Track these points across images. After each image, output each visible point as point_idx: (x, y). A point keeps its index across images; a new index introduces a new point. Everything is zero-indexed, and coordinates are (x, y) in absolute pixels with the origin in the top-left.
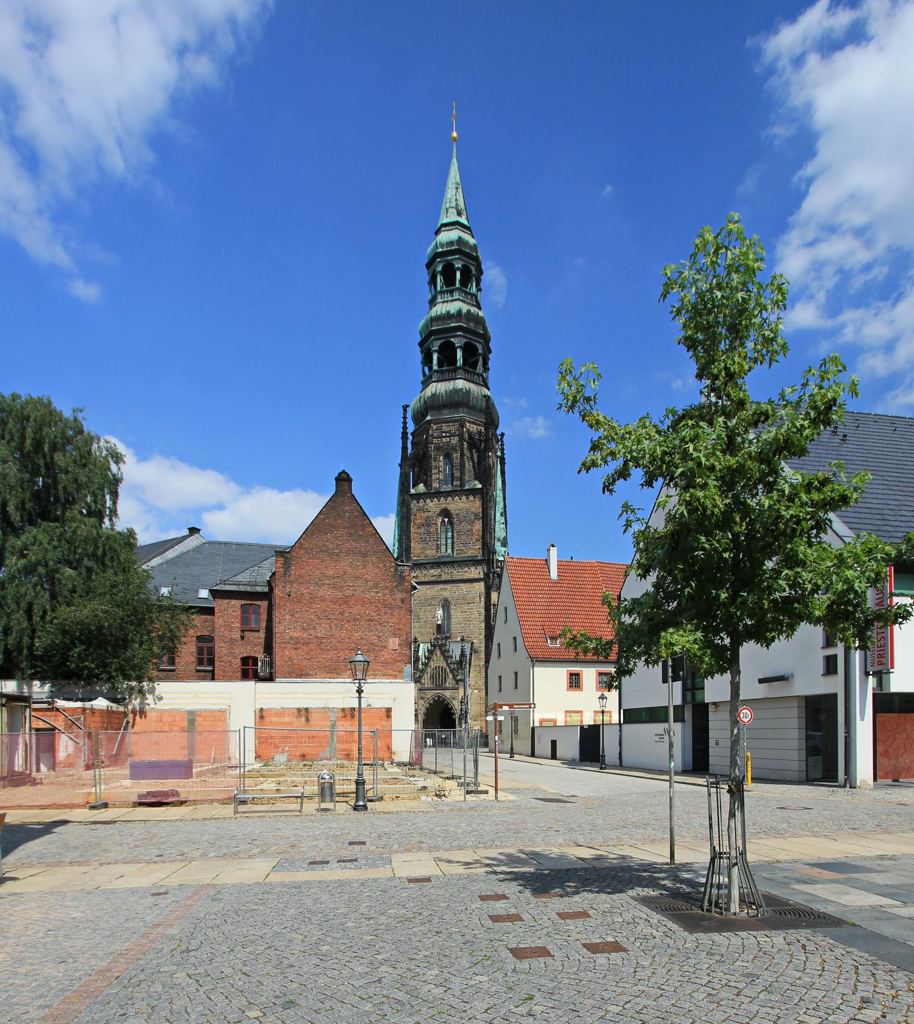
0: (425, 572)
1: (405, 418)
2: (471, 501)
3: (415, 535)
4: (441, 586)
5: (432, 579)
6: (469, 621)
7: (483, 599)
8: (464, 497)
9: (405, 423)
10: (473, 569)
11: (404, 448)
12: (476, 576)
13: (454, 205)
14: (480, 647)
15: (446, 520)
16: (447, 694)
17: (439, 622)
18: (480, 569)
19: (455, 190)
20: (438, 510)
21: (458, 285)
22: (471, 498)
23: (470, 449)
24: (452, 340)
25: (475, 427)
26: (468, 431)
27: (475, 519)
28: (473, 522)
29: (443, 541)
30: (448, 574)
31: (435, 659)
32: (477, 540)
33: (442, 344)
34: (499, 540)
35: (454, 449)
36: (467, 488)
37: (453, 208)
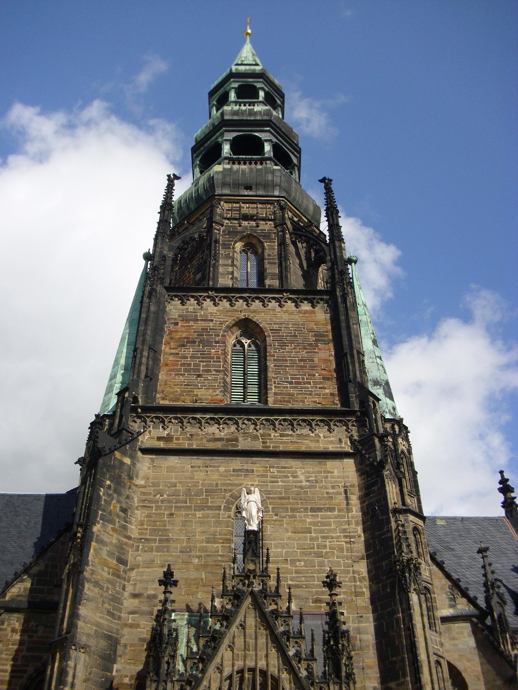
0: (189, 429)
2: (306, 312)
3: (171, 358)
4: (237, 463)
5: (211, 446)
7: (355, 500)
8: (290, 305)
10: (322, 432)
12: (331, 448)
14: (359, 631)
17: (254, 527)
18: (340, 432)
20: (230, 321)
21: (261, 99)
22: (306, 306)
23: (294, 244)
24: (257, 134)
27: (316, 340)
29: (238, 378)
30: (255, 438)
31: (239, 642)
32: (325, 379)
33: (237, 137)
35: (267, 236)
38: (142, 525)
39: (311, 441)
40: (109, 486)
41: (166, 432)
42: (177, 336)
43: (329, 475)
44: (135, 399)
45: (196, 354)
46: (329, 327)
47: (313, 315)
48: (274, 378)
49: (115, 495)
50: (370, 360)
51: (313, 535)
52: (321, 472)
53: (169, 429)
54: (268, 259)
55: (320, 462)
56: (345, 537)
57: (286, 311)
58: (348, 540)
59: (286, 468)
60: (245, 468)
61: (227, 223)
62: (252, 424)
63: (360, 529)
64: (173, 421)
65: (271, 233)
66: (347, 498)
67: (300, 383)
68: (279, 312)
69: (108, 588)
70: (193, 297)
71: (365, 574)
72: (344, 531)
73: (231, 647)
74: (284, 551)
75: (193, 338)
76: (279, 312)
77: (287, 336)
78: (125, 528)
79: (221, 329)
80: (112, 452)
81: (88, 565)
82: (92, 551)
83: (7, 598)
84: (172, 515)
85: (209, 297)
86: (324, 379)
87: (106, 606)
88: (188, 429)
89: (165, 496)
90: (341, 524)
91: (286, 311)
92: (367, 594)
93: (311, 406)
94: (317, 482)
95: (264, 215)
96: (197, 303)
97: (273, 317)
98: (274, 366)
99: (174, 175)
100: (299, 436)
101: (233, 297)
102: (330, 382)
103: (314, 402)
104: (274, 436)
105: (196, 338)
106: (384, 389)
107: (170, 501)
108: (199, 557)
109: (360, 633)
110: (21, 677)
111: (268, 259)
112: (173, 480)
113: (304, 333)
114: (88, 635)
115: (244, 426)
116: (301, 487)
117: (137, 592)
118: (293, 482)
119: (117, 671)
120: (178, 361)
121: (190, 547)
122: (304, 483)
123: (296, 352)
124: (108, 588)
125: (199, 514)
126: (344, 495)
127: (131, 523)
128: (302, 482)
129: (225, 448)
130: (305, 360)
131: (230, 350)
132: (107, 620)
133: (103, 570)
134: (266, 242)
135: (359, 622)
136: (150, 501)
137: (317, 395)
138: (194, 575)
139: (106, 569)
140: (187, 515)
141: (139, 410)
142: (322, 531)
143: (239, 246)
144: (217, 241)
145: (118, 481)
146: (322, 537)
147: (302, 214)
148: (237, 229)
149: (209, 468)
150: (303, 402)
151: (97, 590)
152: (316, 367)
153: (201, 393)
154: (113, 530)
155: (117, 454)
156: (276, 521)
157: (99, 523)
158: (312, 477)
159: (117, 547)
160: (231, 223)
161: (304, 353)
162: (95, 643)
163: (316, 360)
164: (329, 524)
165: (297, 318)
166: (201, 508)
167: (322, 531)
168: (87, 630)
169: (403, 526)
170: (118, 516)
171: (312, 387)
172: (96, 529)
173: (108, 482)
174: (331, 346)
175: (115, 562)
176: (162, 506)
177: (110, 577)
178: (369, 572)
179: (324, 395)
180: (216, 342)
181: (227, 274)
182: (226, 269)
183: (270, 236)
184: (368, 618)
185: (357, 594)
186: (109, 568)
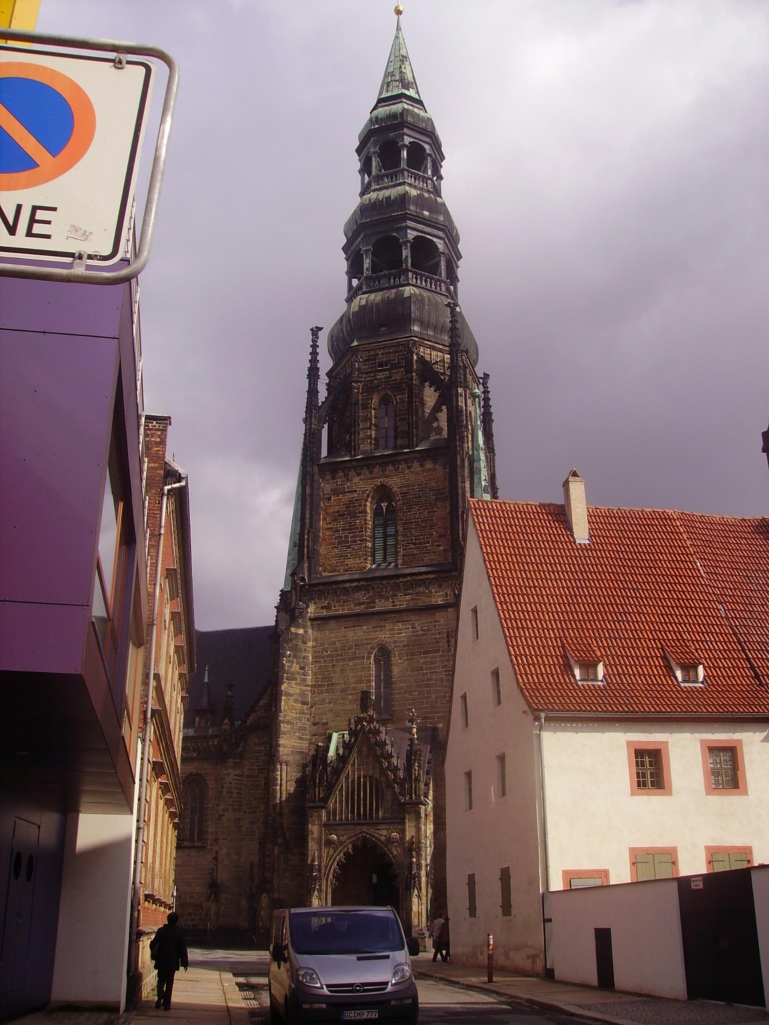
1: (314, 346)
2: (429, 470)
6: (428, 686)
8: (416, 464)
9: (314, 354)
11: (312, 392)
15: (384, 505)
16: (382, 833)
21: (403, 165)
22: (429, 465)
25: (434, 353)
26: (421, 359)
38: (316, 675)
40: (290, 654)
41: (327, 602)
42: (330, 511)
43: (437, 623)
44: (303, 579)
45: (345, 526)
46: (447, 484)
47: (434, 473)
48: (403, 541)
49: (295, 660)
52: (431, 622)
53: (328, 599)
54: (400, 415)
56: (445, 671)
57: (413, 472)
59: (407, 621)
60: (380, 624)
62: (385, 587)
64: (331, 591)
66: (448, 641)
67: (421, 543)
68: (407, 474)
69: (297, 722)
70: (341, 469)
73: (353, 765)
74: (405, 685)
75: (343, 511)
76: (407, 474)
77: (413, 498)
78: (305, 680)
79: (363, 499)
80: (288, 629)
81: (281, 712)
82: (283, 702)
83: (248, 724)
84: (334, 665)
85: (352, 467)
86: (439, 536)
87: (297, 734)
88: (341, 597)
89: (329, 652)
91: (413, 472)
93: (429, 563)
94: (428, 630)
96: (344, 475)
97: (401, 480)
98: (403, 530)
99: (316, 327)
101: (371, 464)
102: (443, 539)
103: (431, 559)
104: (400, 596)
105: (345, 511)
107: (332, 656)
108: (352, 694)
110: (264, 772)
111: (400, 415)
112: (333, 640)
113: (426, 493)
114: (287, 755)
115: (379, 590)
116: (417, 636)
117: (316, 721)
119: (308, 772)
120: (333, 535)
121: (346, 688)
123: (420, 513)
124: (297, 722)
125: (351, 663)
126: (446, 639)
127: (308, 675)
128: (418, 631)
129: (366, 611)
132: (298, 742)
133: (293, 713)
136: (320, 657)
138: (350, 707)
139: (294, 711)
140: (343, 665)
141: (307, 587)
143: (375, 401)
144: (356, 403)
145: (295, 649)
147: (435, 343)
149: (356, 628)
151: (289, 726)
153: (349, 562)
154: (296, 684)
155: (293, 629)
156: (400, 663)
157: (285, 683)
158: (425, 627)
159: (300, 695)
162: (292, 758)
163: (434, 518)
166: (351, 659)
167: (430, 668)
168: (286, 752)
170: (298, 673)
171: (430, 546)
172: (283, 687)
173: (289, 652)
174: (448, 503)
175: (300, 705)
176: (327, 660)
177: (298, 715)
181: (366, 439)
182: (365, 432)
186: (295, 709)
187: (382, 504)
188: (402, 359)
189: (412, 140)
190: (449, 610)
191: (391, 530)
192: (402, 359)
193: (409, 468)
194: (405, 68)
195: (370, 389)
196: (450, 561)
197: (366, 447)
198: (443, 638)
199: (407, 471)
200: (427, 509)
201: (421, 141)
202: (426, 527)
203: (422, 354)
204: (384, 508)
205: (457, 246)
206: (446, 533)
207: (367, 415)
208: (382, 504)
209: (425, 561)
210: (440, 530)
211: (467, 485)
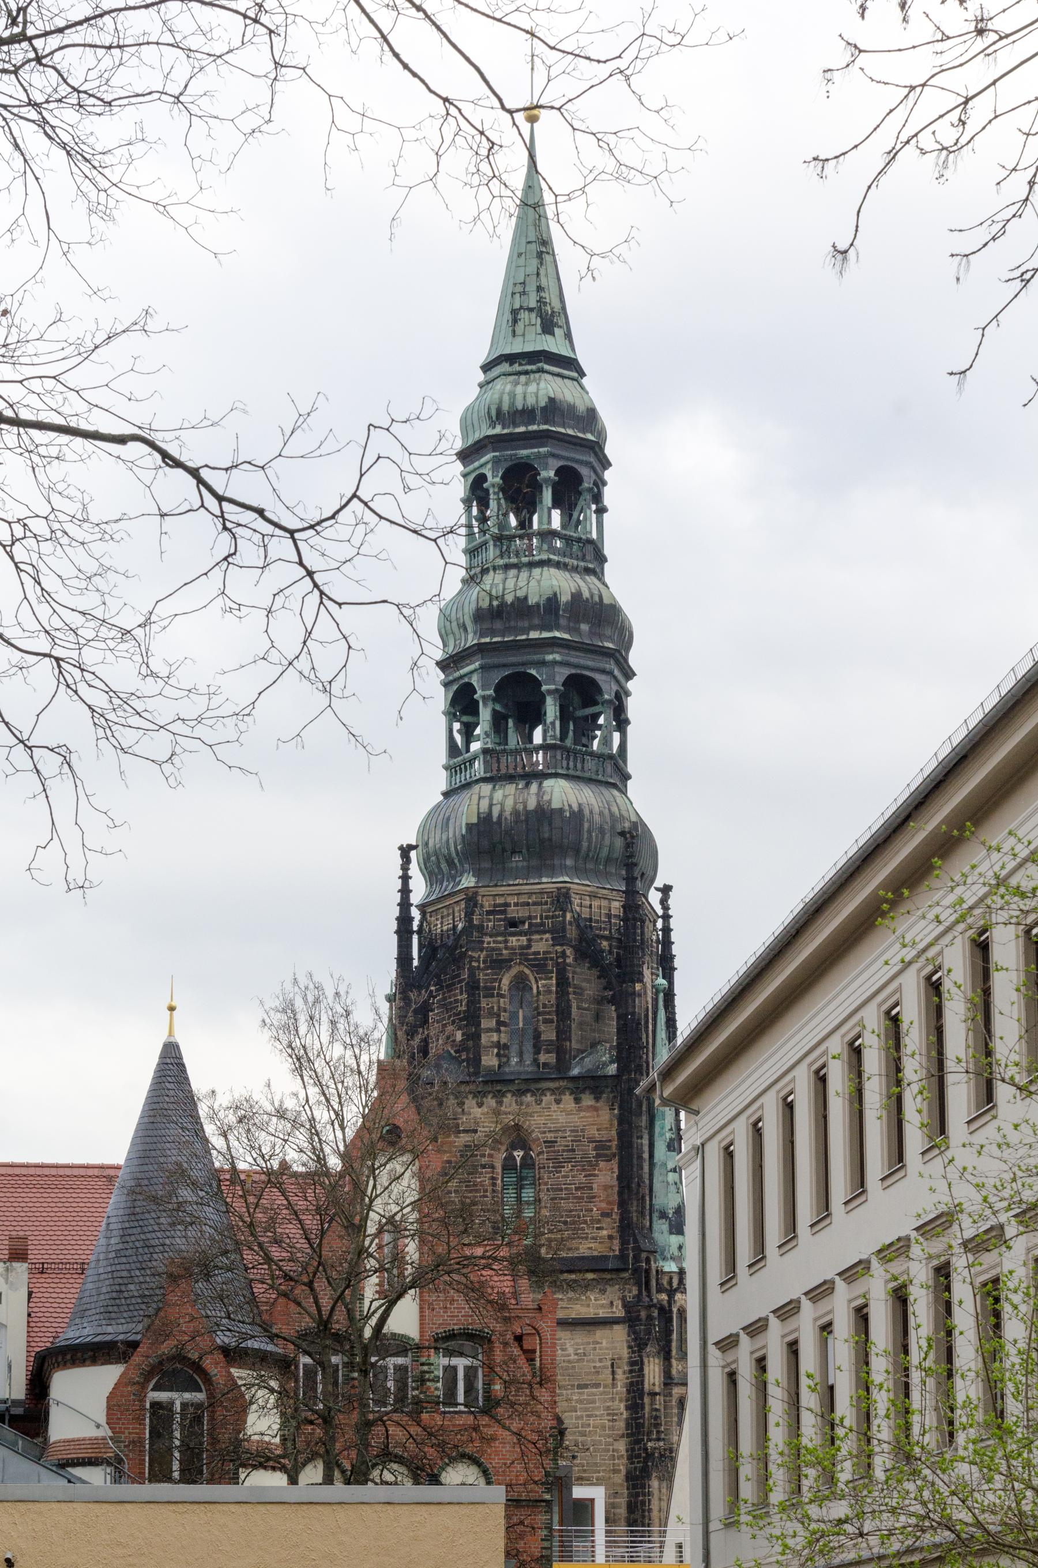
6: (583, 1434)
7: (620, 1375)
8: (568, 1099)
12: (602, 1313)
13: (533, 304)
15: (518, 1154)
19: (535, 262)
22: (588, 1100)
24: (533, 672)
25: (596, 903)
27: (598, 1156)
28: (594, 1166)
32: (605, 1215)
34: (663, 1215)
36: (575, 1072)
37: (531, 310)
39: (582, 1305)
46: (614, 1133)
50: (660, 1178)
51: (579, 1413)
52: (589, 1343)
55: (589, 1331)
56: (608, 1414)
58: (610, 1418)
61: (489, 943)
63: (622, 1406)
65: (546, 959)
66: (613, 1373)
67: (574, 1222)
71: (624, 1453)
72: (608, 1408)
77: (564, 1151)
90: (605, 1401)
92: (624, 1472)
94: (585, 1354)
95: (539, 921)
100: (570, 1299)
101: (499, 1091)
106: (670, 1225)
109: (614, 1508)
116: (569, 1361)
118: (563, 1355)
122: (573, 1357)
123: (573, 1177)
130: (583, 1188)
131: (499, 1170)
134: (541, 979)
135: (615, 1497)
137: (593, 1238)
142: (586, 1410)
146: (588, 1416)
148: (501, 954)
150: (577, 1249)
152: (594, 1197)
160: (494, 942)
161: (582, 1178)
163: (595, 1186)
164: (594, 1402)
165: (577, 1120)
167: (586, 1410)
169: (657, 1410)
174: (615, 1164)
178: (627, 1451)
179: (601, 1238)
180: (484, 1167)
183: (546, 965)
184: (622, 1494)
185: (615, 1471)
187: (515, 1153)
188: (547, 917)
189: (561, 463)
190: (616, 1327)
191: (528, 1194)
192: (547, 917)
193: (558, 1102)
194: (546, 275)
195: (499, 964)
196: (617, 1253)
197: (491, 1060)
198: (605, 1367)
199: (554, 1107)
200: (584, 1170)
201: (577, 461)
202: (582, 1198)
203: (578, 909)
204: (518, 1159)
205: (626, 660)
206: (612, 1209)
207: (493, 1007)
208: (515, 1153)
209: (582, 1251)
210: (603, 1205)
211: (645, 1141)
